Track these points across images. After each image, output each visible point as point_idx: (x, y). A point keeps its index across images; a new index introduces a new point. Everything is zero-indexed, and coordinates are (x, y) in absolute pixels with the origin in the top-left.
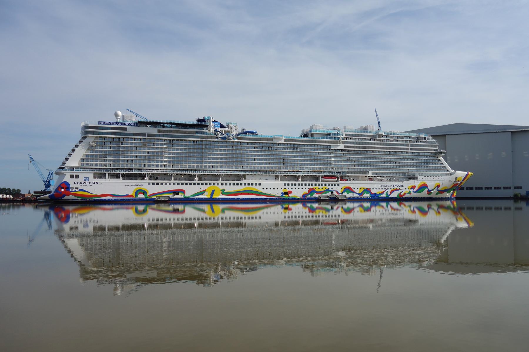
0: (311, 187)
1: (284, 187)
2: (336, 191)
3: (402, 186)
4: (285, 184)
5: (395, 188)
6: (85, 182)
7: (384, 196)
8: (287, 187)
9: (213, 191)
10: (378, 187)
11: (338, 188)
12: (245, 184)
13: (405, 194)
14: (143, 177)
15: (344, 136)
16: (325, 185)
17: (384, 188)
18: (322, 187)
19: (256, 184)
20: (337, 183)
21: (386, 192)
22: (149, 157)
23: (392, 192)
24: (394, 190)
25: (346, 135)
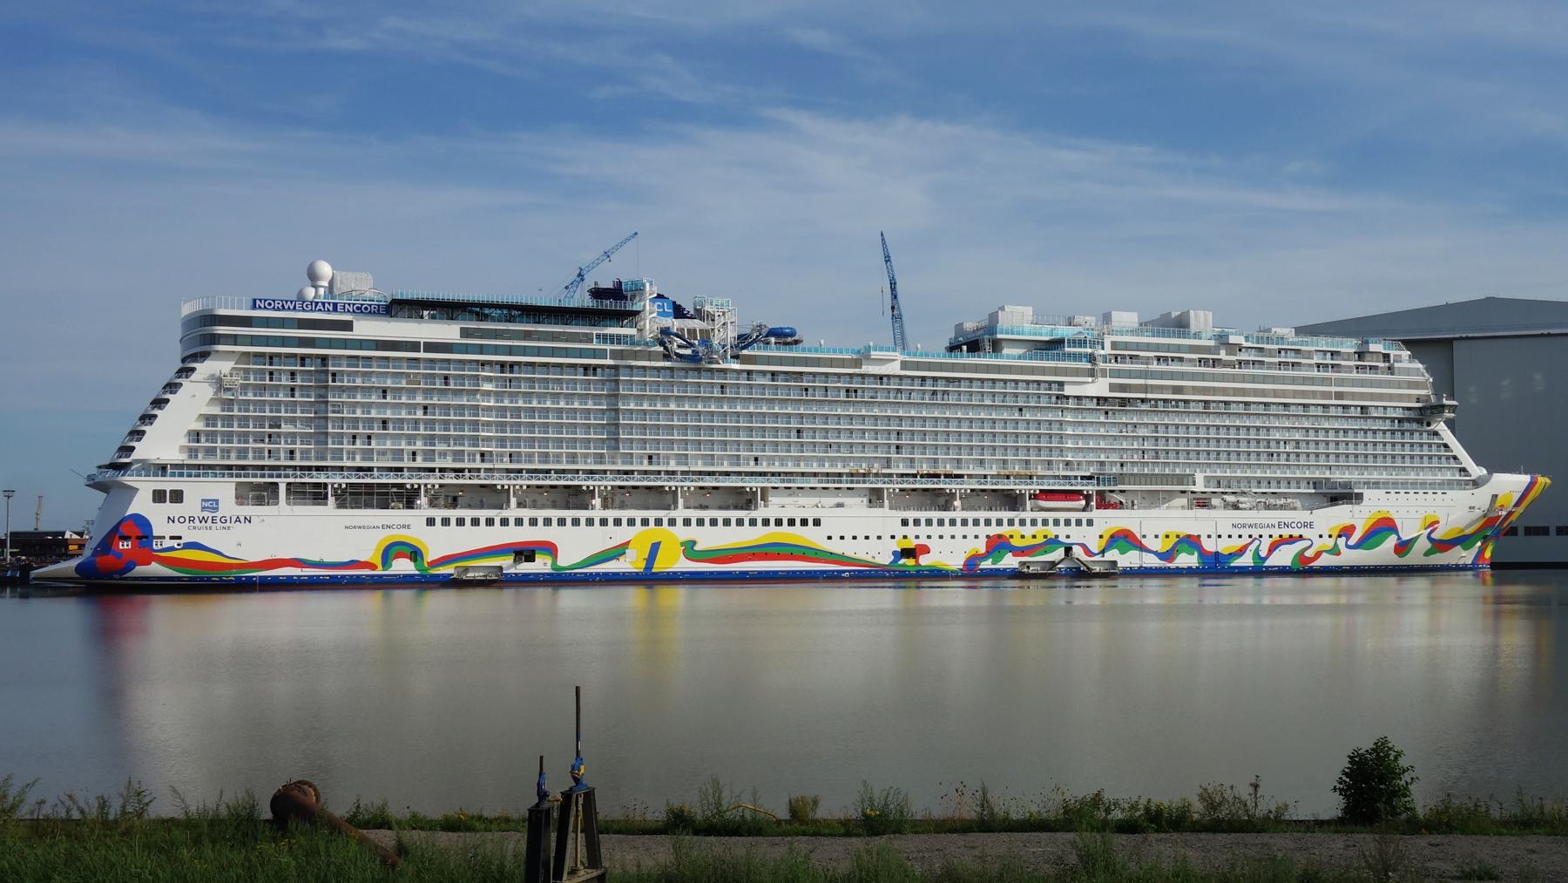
0: (994, 530)
1: (901, 531)
2: (1083, 546)
3: (1311, 525)
4: (905, 523)
5: (1286, 533)
6: (206, 514)
7: (1246, 560)
8: (911, 530)
9: (655, 548)
11: (1088, 533)
12: (766, 522)
13: (1318, 555)
14: (408, 498)
15: (1108, 350)
17: (1245, 532)
20: (1084, 516)
21: (1253, 547)
22: (430, 424)
23: (1273, 548)
25: (1114, 345)
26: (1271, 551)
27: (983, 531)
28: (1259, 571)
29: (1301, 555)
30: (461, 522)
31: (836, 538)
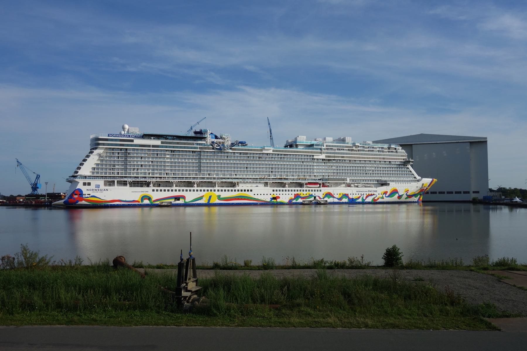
0: (296, 193)
2: (319, 197)
3: (376, 191)
4: (273, 191)
5: (370, 193)
7: (360, 200)
8: (275, 193)
9: (210, 197)
11: (320, 193)
12: (238, 191)
13: (378, 199)
14: (148, 184)
15: (325, 147)
16: (309, 191)
17: (360, 193)
18: (306, 193)
19: (248, 191)
20: (319, 189)
22: (153, 166)
23: (367, 197)
24: (369, 195)
25: (327, 146)
26: (366, 198)
27: (293, 193)
28: (363, 203)
29: (374, 199)
31: (256, 194)
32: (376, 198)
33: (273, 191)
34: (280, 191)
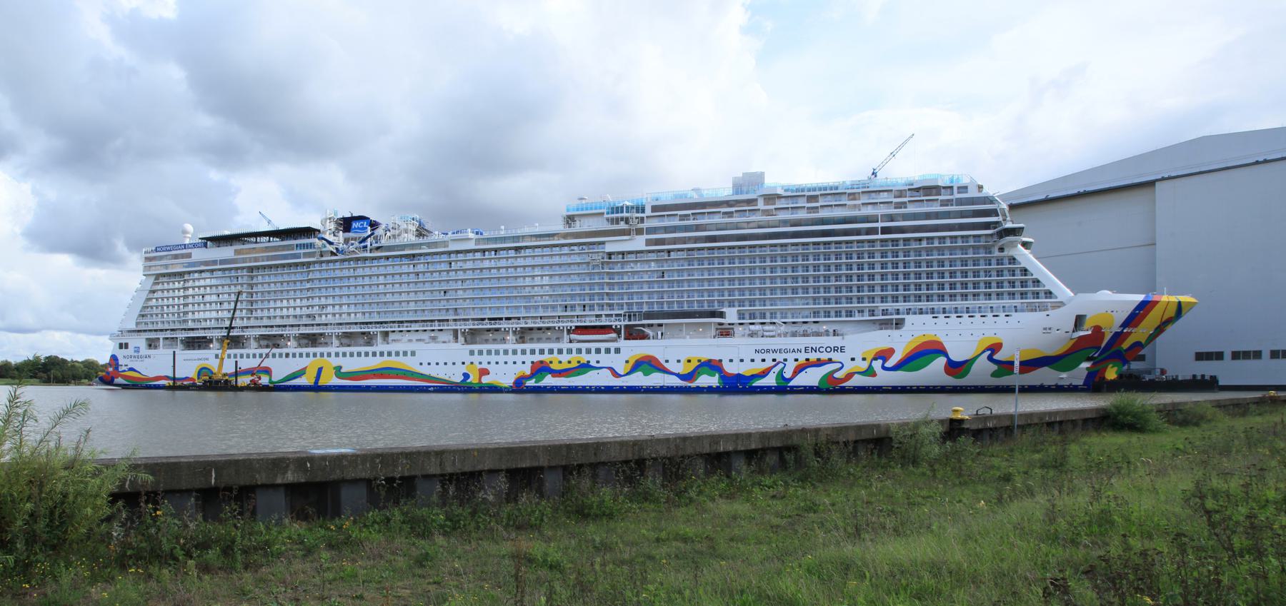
0: (537, 357)
1: (468, 359)
4: (472, 353)
5: (813, 357)
8: (476, 359)
9: (320, 370)
10: (748, 354)
12: (382, 354)
16: (579, 351)
17: (769, 357)
18: (569, 357)
19: (405, 353)
20: (612, 345)
21: (777, 369)
23: (799, 370)
24: (809, 364)
27: (529, 358)
30: (359, 354)
31: (425, 364)
32: (837, 375)
33: (472, 353)
34: (489, 352)
